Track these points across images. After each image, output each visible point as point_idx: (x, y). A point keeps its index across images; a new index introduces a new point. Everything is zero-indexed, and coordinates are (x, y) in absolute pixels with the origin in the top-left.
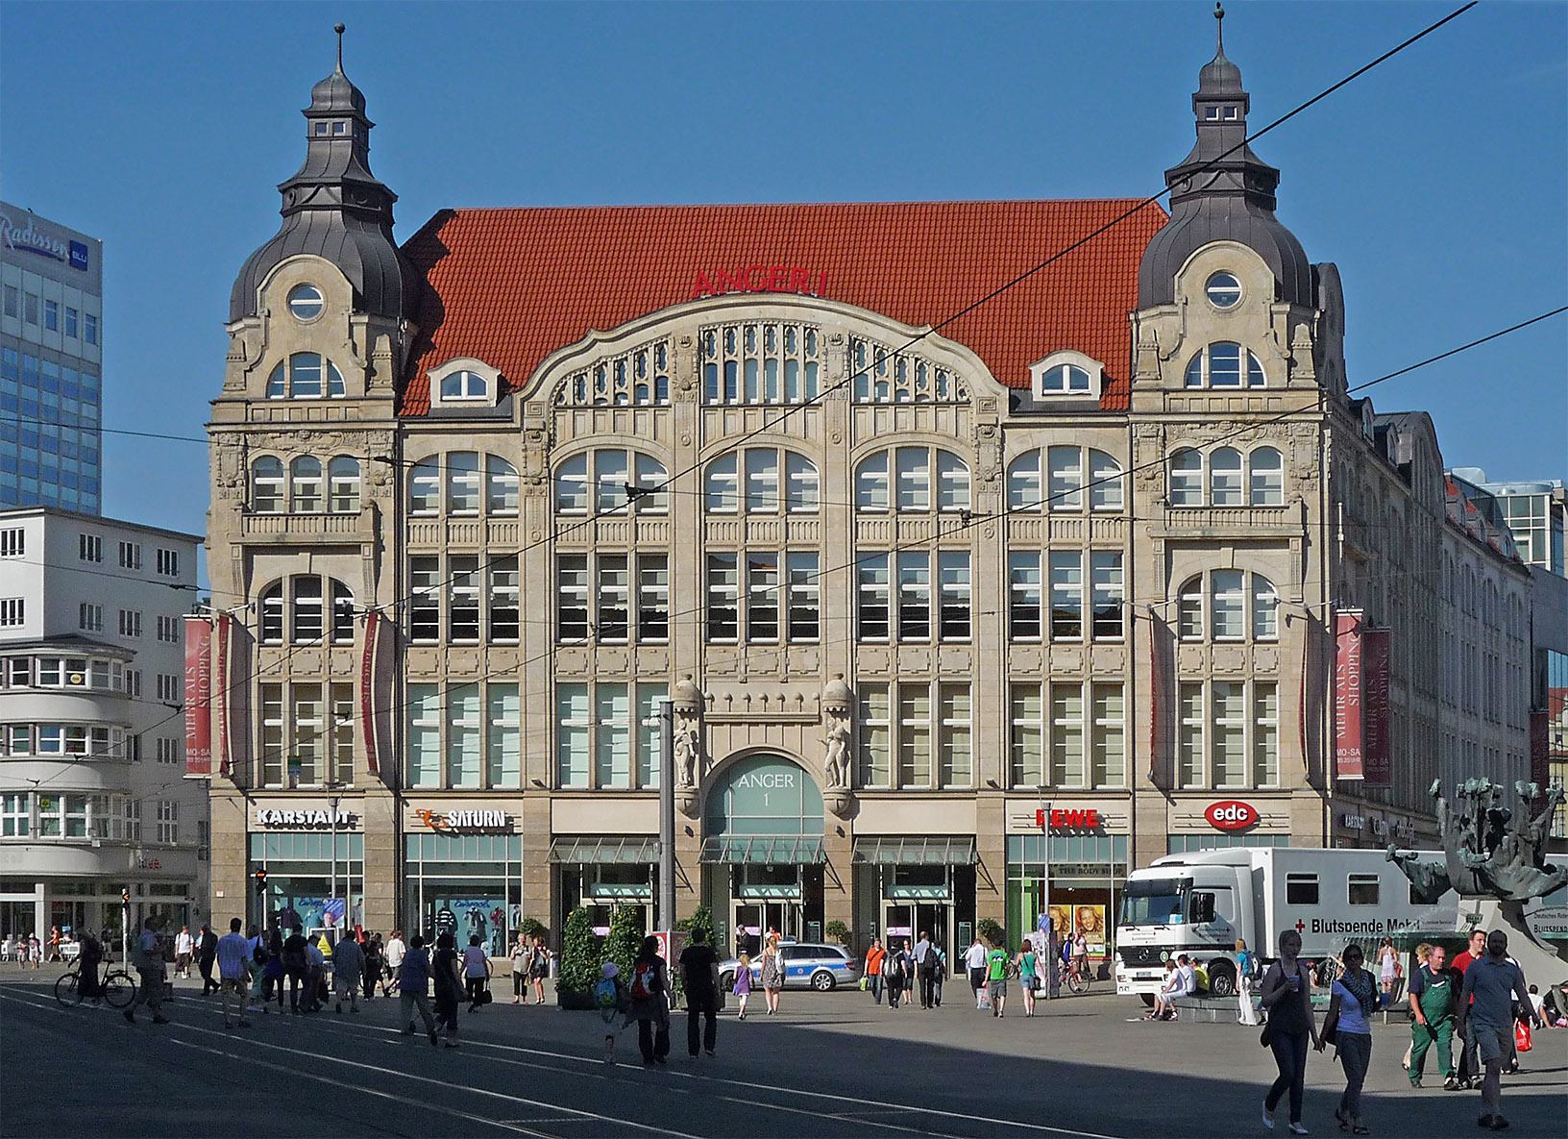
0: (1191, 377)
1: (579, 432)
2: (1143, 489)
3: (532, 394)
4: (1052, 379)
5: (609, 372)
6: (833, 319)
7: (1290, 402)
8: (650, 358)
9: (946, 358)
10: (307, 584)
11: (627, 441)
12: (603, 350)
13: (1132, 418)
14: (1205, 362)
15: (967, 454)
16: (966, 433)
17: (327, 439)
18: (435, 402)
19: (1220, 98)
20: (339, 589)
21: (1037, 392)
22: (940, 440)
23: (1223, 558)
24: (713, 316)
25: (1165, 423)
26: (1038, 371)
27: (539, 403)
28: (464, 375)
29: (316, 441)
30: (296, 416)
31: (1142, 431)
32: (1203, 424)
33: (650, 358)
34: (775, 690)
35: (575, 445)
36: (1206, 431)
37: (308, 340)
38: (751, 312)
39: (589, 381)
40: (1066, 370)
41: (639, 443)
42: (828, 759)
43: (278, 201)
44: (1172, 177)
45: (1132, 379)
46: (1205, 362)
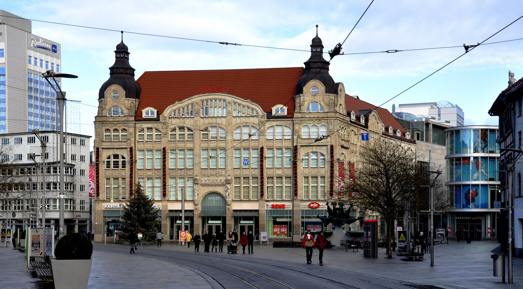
1: (176, 123)
2: (295, 135)
4: (277, 111)
5: (181, 109)
6: (229, 98)
7: (329, 115)
8: (190, 107)
9: (253, 106)
10: (116, 156)
11: (185, 125)
12: (180, 105)
16: (257, 123)
17: (120, 125)
18: (143, 117)
20: (123, 157)
23: (314, 149)
24: (203, 98)
26: (274, 109)
30: (113, 120)
32: (309, 120)
33: (190, 107)
34: (216, 178)
36: (309, 122)
38: (211, 97)
42: (227, 194)
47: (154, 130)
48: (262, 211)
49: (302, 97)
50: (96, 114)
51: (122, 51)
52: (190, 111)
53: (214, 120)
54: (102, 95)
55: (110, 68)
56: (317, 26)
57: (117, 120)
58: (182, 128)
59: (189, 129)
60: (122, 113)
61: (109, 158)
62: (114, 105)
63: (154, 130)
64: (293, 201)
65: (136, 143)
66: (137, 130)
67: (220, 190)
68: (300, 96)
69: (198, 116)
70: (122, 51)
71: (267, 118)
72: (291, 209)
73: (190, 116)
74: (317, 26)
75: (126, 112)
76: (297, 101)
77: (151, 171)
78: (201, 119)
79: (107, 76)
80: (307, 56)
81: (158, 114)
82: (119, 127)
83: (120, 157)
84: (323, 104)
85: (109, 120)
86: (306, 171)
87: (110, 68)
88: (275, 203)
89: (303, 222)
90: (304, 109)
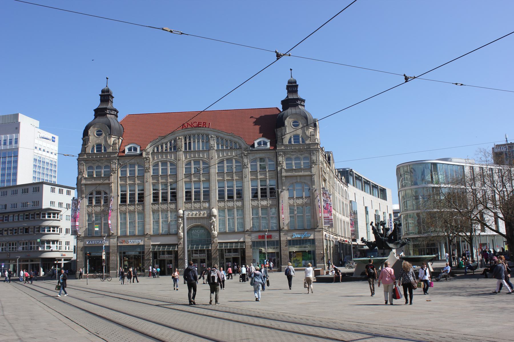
10: (99, 193)
14: (292, 139)
19: (292, 87)
20: (106, 193)
27: (149, 152)
32: (292, 152)
36: (292, 153)
39: (160, 148)
43: (94, 113)
44: (283, 102)
45: (276, 143)
46: (292, 139)
48: (248, 242)
49: (284, 130)
50: (80, 152)
52: (173, 146)
54: (86, 133)
55: (95, 110)
61: (91, 194)
62: (97, 142)
67: (204, 223)
68: (282, 130)
72: (278, 239)
74: (291, 70)
76: (279, 134)
79: (90, 117)
80: (284, 95)
81: (141, 151)
82: (102, 163)
83: (103, 193)
87: (95, 110)
89: (290, 252)
90: (286, 141)
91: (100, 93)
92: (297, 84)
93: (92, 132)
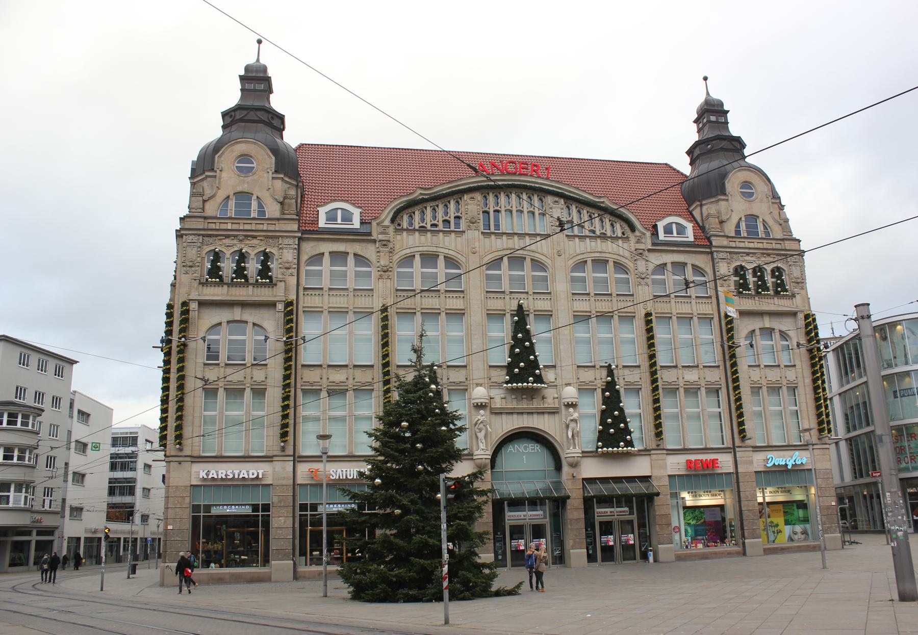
0: (738, 232)
3: (383, 221)
4: (668, 230)
13: (714, 249)
14: (743, 226)
15: (630, 264)
17: (255, 242)
21: (662, 236)
22: (615, 257)
23: (767, 323)
25: (730, 253)
26: (660, 225)
28: (339, 212)
29: (248, 242)
30: (235, 227)
31: (721, 255)
32: (748, 254)
35: (408, 251)
37: (246, 185)
40: (674, 226)
41: (447, 251)
46: (743, 226)
47: (351, 260)
51: (256, 81)
53: (516, 243)
55: (225, 115)
56: (705, 79)
57: (247, 227)
58: (429, 258)
59: (451, 262)
60: (262, 212)
62: (239, 189)
63: (351, 260)
64: (733, 450)
65: (301, 292)
66: (304, 258)
69: (477, 229)
70: (256, 81)
71: (653, 244)
73: (452, 228)
74: (705, 79)
75: (273, 210)
77: (343, 371)
78: (481, 237)
79: (214, 131)
84: (770, 222)
85: (223, 226)
86: (755, 375)
88: (693, 457)
91: (243, 73)
92: (726, 108)
93: (226, 162)
